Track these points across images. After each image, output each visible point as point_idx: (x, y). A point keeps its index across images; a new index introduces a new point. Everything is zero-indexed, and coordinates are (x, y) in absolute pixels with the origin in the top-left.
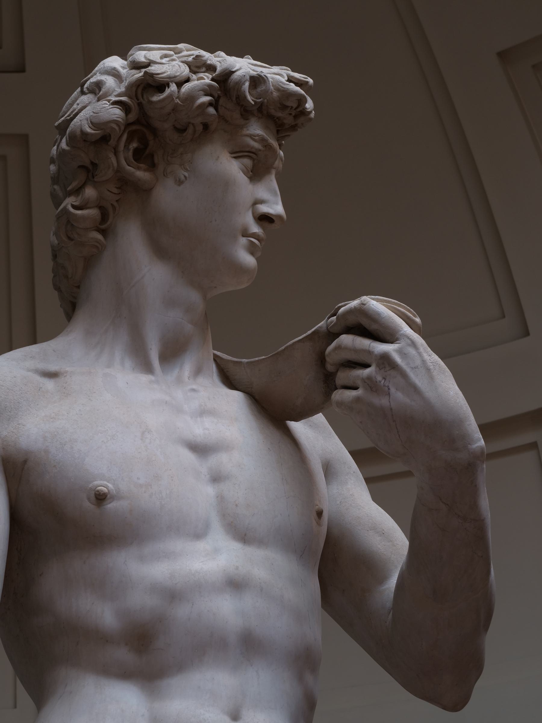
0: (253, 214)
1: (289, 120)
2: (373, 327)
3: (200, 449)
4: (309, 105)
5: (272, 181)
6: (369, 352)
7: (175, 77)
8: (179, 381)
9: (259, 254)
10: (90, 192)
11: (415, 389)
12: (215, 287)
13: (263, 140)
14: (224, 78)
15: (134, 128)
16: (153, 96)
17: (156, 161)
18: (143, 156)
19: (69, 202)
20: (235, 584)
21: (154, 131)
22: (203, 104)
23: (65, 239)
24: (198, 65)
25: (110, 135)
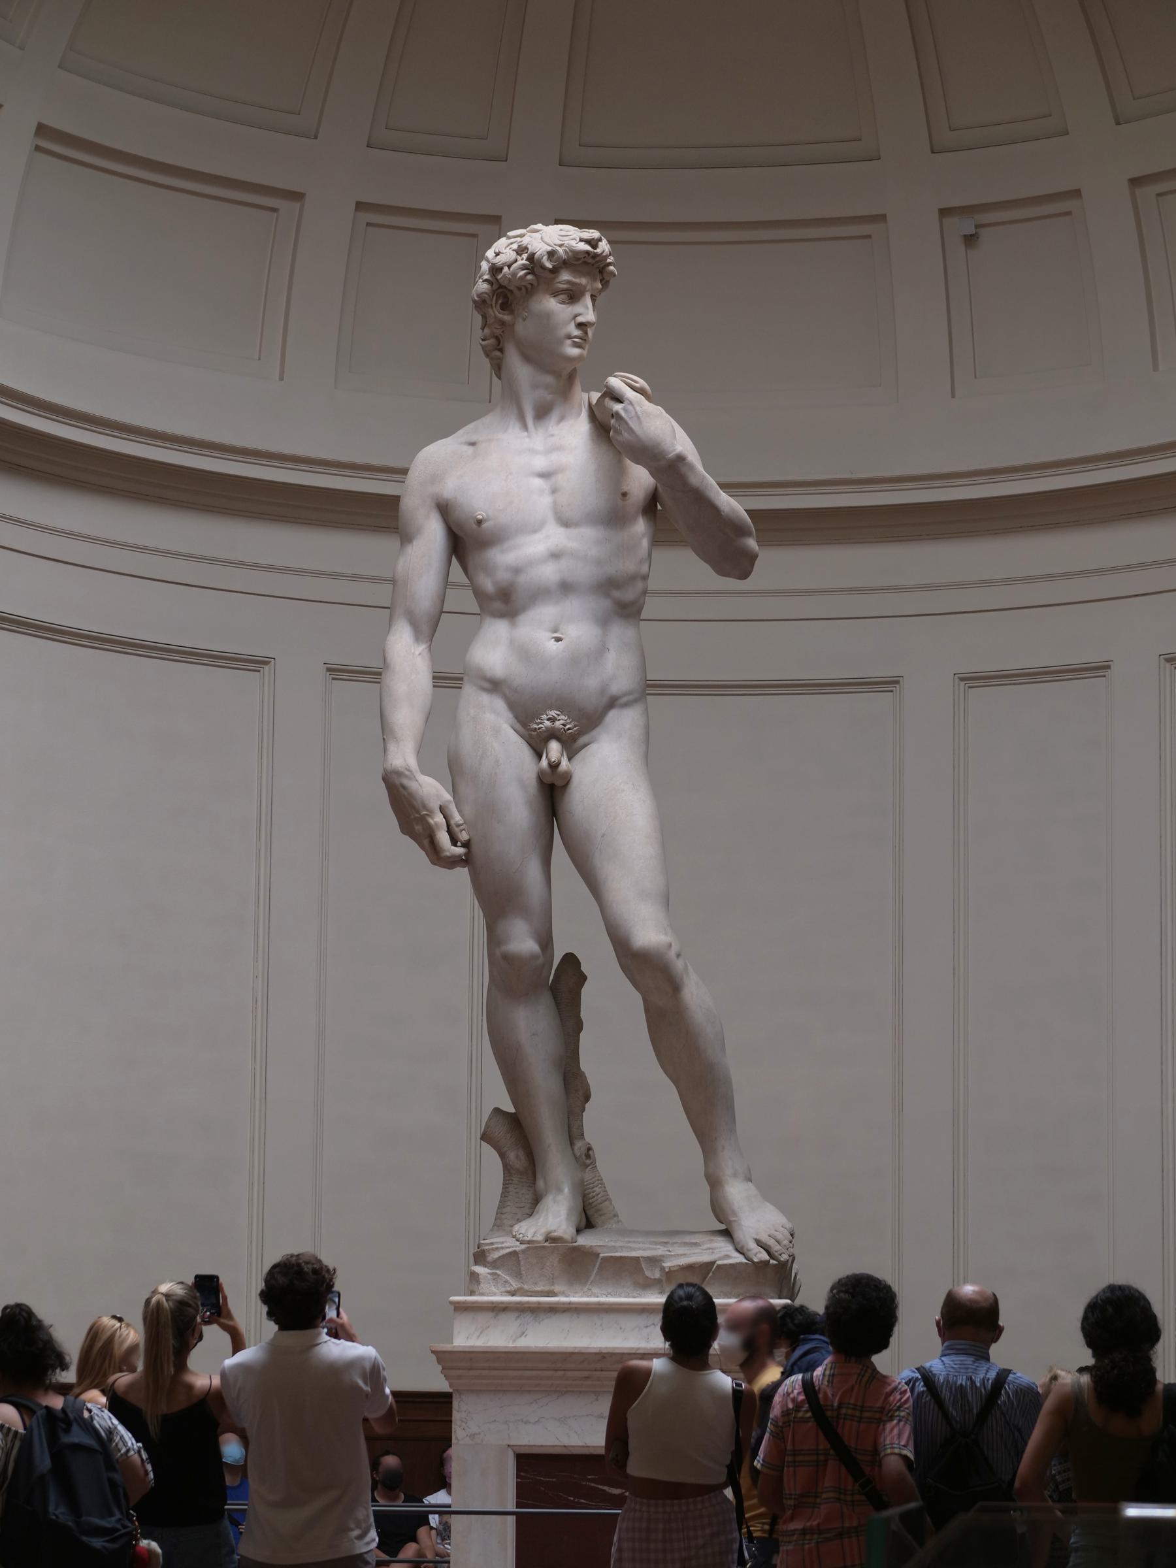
3: (545, 475)
10: (487, 331)
13: (568, 282)
14: (531, 258)
18: (506, 306)
20: (555, 555)
21: (511, 291)
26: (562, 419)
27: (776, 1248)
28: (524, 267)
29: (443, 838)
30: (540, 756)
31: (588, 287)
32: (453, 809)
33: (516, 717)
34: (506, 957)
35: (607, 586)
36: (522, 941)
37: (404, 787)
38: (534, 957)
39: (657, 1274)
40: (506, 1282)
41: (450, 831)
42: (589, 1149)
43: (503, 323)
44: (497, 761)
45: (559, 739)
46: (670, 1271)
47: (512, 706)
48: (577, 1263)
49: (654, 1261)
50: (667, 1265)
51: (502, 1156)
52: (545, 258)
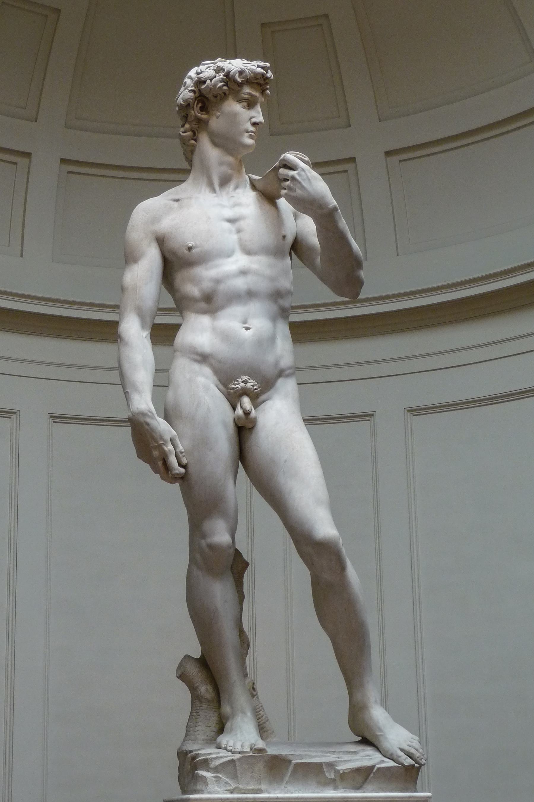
1: (262, 82)
2: (289, 165)
3: (231, 221)
4: (270, 74)
5: (258, 108)
6: (287, 175)
8: (228, 193)
9: (255, 138)
10: (187, 126)
13: (249, 94)
14: (227, 75)
15: (199, 98)
18: (203, 109)
20: (243, 273)
21: (207, 98)
26: (236, 187)
27: (417, 754)
28: (222, 80)
29: (173, 460)
30: (234, 408)
31: (259, 100)
32: (178, 441)
33: (220, 381)
34: (211, 547)
35: (277, 295)
36: (220, 536)
37: (148, 424)
38: (229, 547)
39: (332, 776)
40: (227, 783)
41: (176, 456)
42: (254, 684)
43: (199, 121)
44: (209, 409)
45: (248, 395)
46: (344, 773)
47: (216, 372)
48: (277, 767)
49: (331, 765)
50: (341, 768)
51: (193, 689)
52: (237, 75)
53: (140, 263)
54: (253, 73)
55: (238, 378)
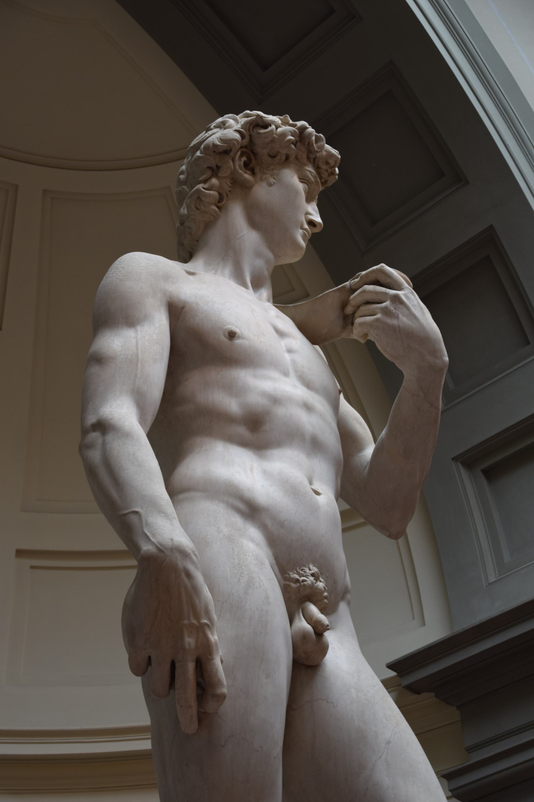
0: (305, 219)
6: (386, 294)
7: (275, 122)
10: (214, 181)
11: (415, 317)
12: (280, 257)
16: (260, 130)
17: (256, 171)
19: (200, 186)
20: (308, 407)
22: (290, 140)
23: (194, 209)
24: (286, 121)
25: (231, 150)
37: (189, 575)
44: (267, 598)
53: (139, 328)
54: (326, 151)
55: (306, 567)
